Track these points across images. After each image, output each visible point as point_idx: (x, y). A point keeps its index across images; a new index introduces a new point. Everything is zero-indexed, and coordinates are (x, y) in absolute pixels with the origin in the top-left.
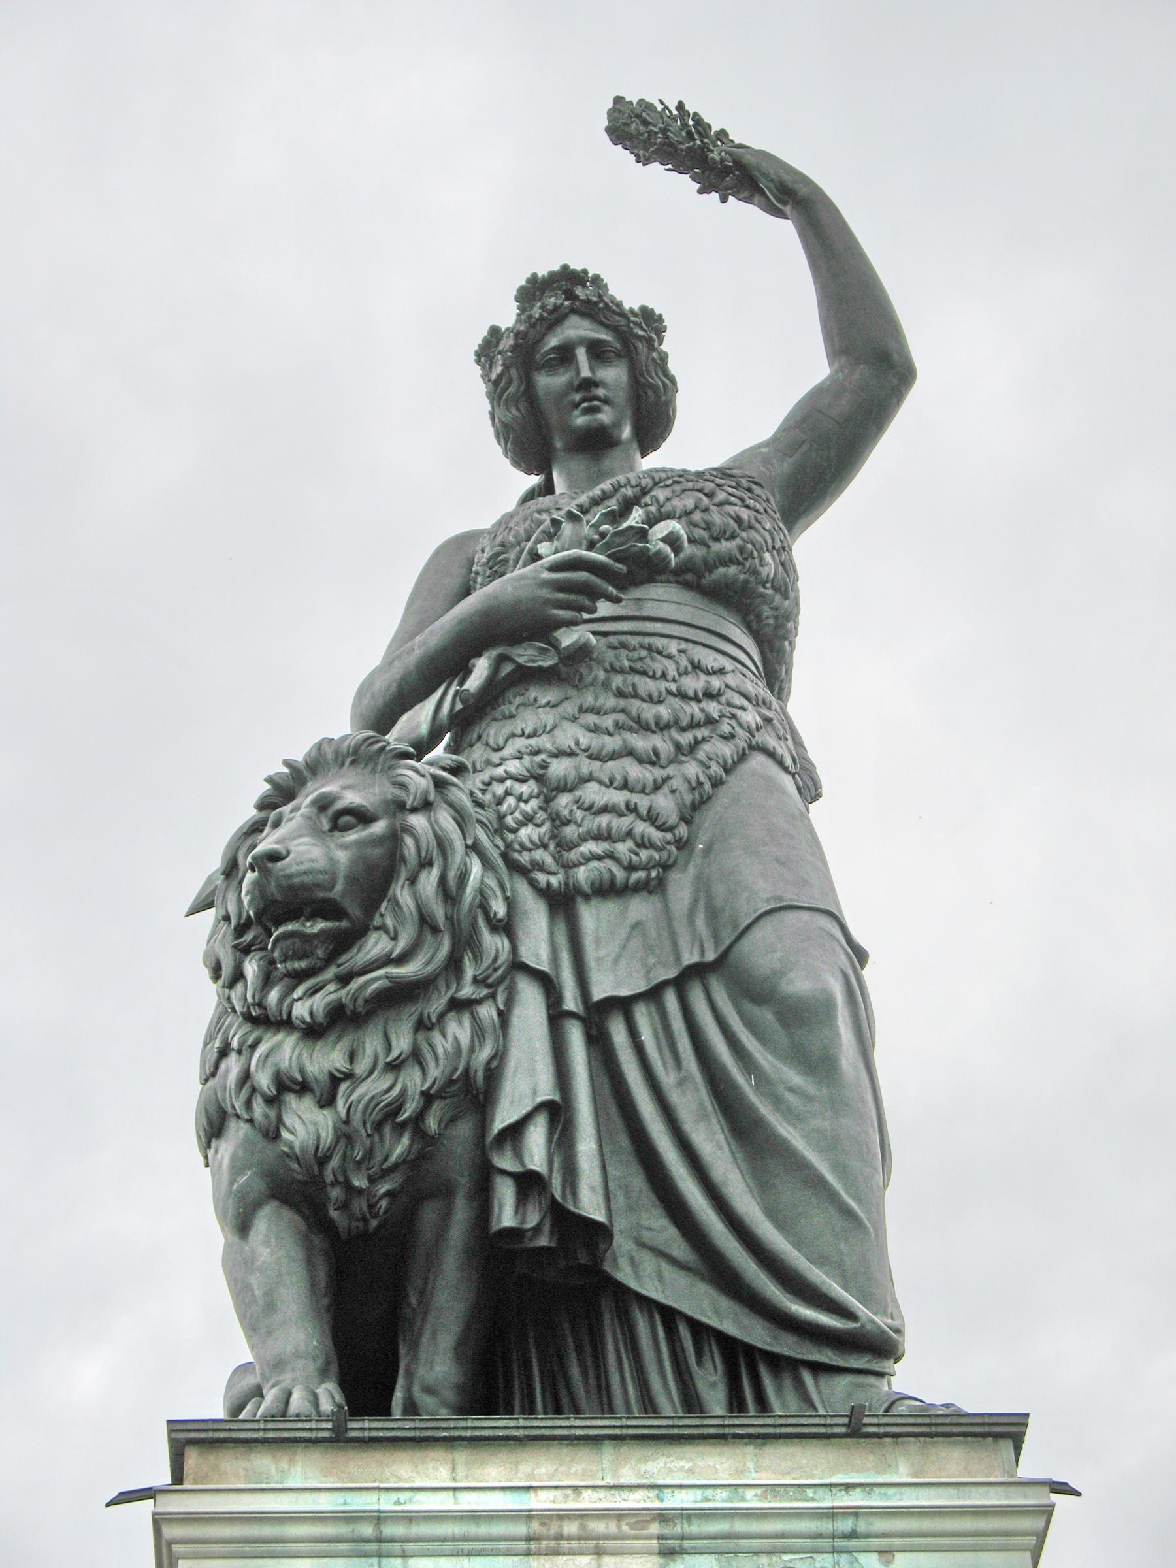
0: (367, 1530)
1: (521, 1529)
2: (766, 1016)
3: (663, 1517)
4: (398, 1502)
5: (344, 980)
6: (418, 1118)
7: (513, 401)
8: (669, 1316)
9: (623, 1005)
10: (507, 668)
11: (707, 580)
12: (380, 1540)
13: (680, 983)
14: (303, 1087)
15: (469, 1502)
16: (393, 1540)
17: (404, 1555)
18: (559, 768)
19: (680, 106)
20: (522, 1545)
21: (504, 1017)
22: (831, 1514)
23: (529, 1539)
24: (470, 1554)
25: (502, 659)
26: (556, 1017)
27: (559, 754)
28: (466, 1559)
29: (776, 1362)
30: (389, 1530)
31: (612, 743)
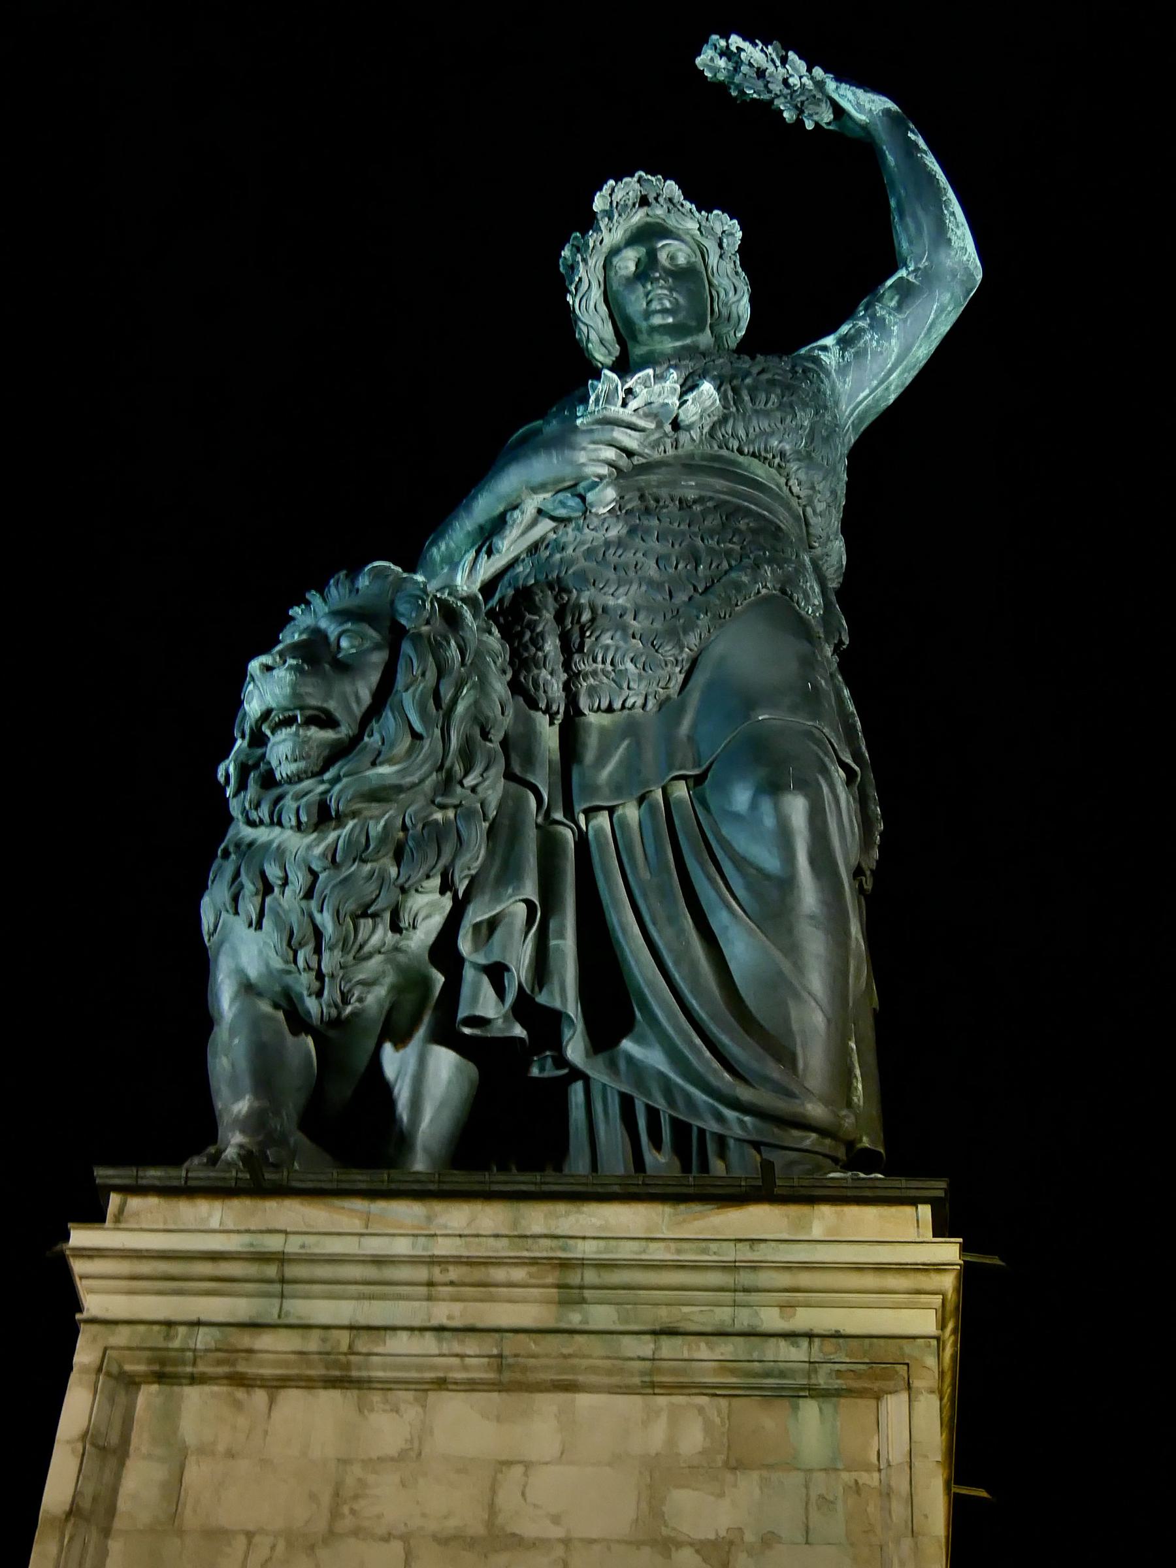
1: (422, 1274)
3: (565, 1265)
4: (303, 1246)
12: (283, 1281)
15: (374, 1246)
16: (295, 1281)
17: (307, 1297)
20: (423, 1290)
22: (731, 1267)
23: (430, 1284)
24: (372, 1297)
28: (366, 1303)
30: (292, 1271)
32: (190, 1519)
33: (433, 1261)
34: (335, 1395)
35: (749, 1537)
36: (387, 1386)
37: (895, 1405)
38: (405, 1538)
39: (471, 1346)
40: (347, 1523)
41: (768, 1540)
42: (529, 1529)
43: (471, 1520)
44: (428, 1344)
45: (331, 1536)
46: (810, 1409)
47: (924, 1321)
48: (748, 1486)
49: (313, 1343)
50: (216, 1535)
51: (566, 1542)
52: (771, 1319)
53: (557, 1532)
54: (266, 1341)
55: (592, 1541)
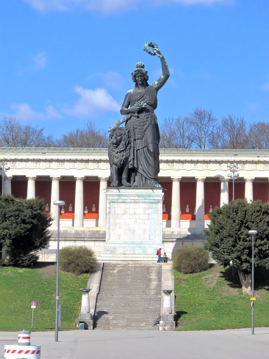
0: (119, 195)
2: (149, 152)
5: (118, 149)
6: (124, 160)
7: (134, 79)
8: (142, 174)
9: (139, 150)
10: (132, 115)
11: (149, 104)
13: (143, 148)
14: (115, 157)
18: (135, 127)
19: (151, 43)
21: (130, 151)
25: (131, 114)
26: (134, 150)
27: (135, 125)
29: (148, 179)
31: (139, 125)
32: (116, 213)
33: (129, 195)
34: (124, 203)
35: (151, 213)
36: (127, 203)
37: (159, 204)
38: (130, 214)
39: (133, 200)
40: (125, 213)
41: (152, 213)
42: (137, 213)
43: (134, 213)
44: (130, 200)
45: (125, 214)
46: (154, 204)
47: (161, 198)
48: (150, 209)
49: (122, 200)
50: (118, 214)
51: (139, 214)
52: (152, 198)
53: (139, 213)
54: (119, 200)
55: (141, 214)
